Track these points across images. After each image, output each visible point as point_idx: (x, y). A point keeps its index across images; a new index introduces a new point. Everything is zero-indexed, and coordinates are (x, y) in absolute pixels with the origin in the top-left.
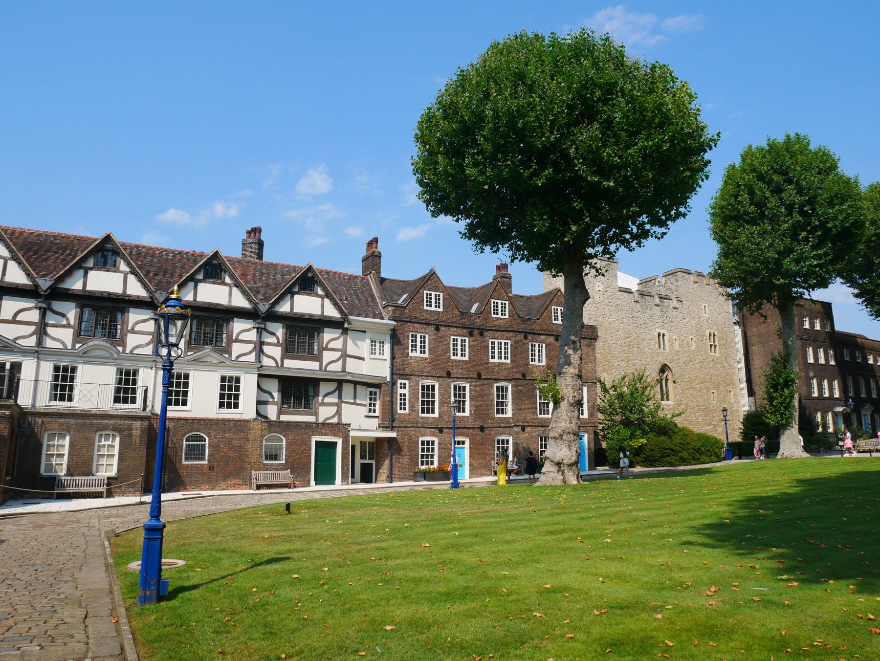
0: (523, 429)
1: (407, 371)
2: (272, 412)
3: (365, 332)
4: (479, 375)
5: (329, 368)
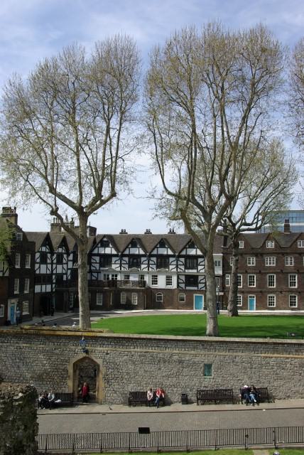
2: (183, 286)
4: (260, 272)
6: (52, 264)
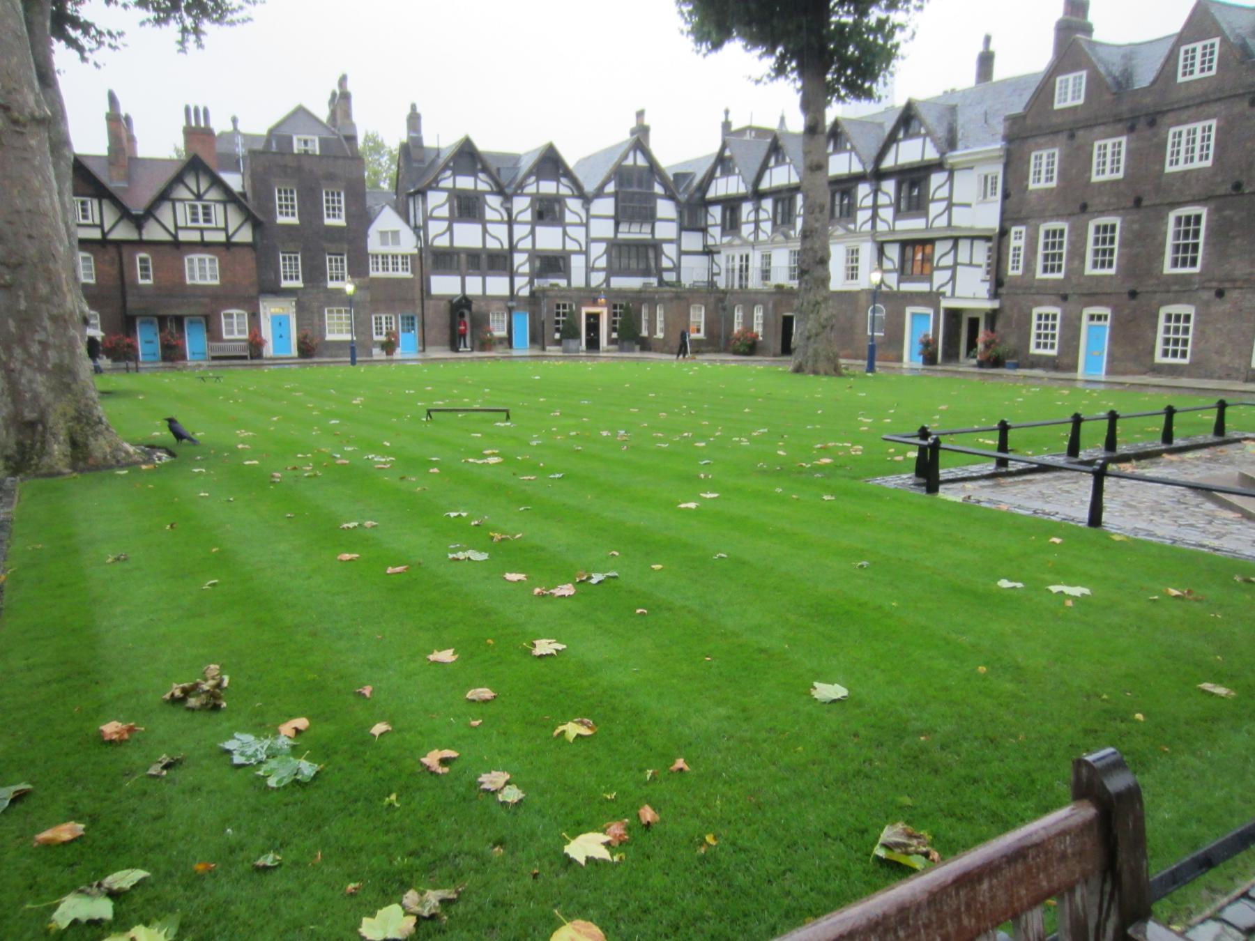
0: (1220, 294)
1: (1024, 213)
2: (892, 280)
3: (971, 168)
4: (1138, 202)
5: (936, 224)
6: (511, 222)
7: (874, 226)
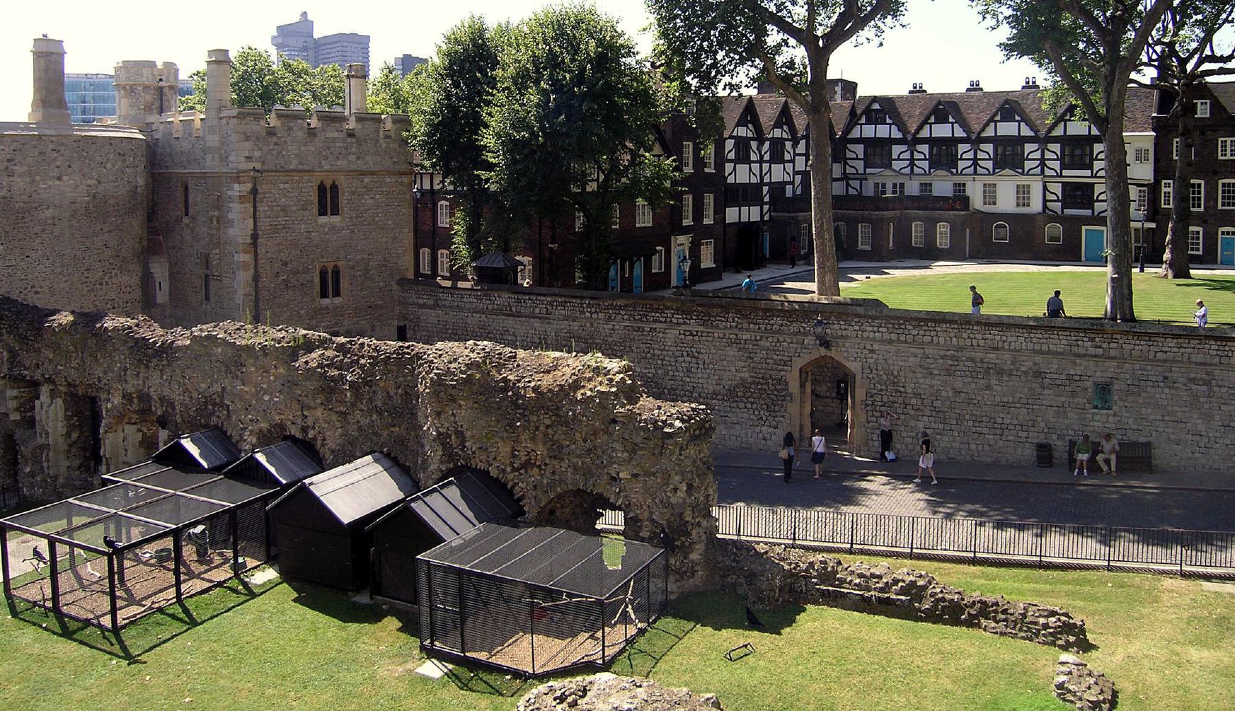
7: (1043, 171)
